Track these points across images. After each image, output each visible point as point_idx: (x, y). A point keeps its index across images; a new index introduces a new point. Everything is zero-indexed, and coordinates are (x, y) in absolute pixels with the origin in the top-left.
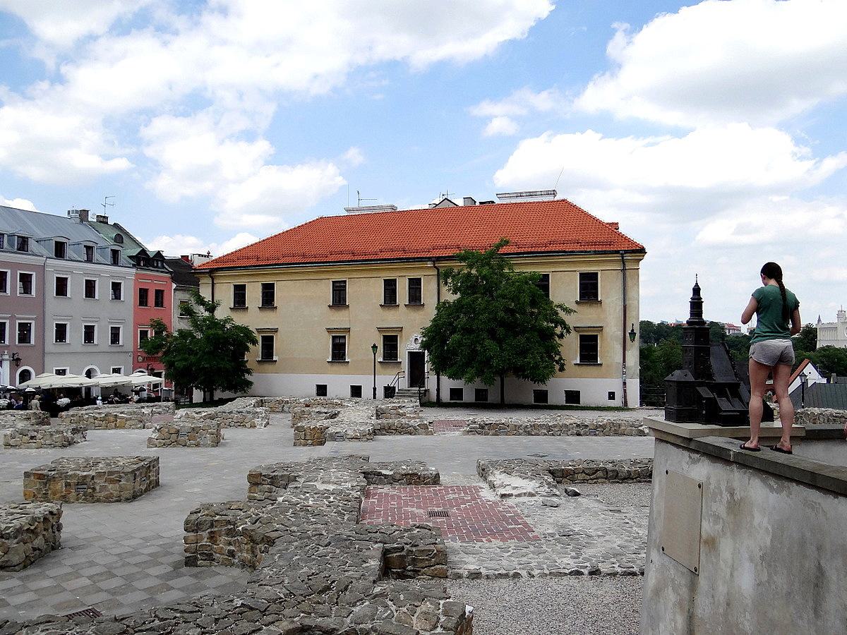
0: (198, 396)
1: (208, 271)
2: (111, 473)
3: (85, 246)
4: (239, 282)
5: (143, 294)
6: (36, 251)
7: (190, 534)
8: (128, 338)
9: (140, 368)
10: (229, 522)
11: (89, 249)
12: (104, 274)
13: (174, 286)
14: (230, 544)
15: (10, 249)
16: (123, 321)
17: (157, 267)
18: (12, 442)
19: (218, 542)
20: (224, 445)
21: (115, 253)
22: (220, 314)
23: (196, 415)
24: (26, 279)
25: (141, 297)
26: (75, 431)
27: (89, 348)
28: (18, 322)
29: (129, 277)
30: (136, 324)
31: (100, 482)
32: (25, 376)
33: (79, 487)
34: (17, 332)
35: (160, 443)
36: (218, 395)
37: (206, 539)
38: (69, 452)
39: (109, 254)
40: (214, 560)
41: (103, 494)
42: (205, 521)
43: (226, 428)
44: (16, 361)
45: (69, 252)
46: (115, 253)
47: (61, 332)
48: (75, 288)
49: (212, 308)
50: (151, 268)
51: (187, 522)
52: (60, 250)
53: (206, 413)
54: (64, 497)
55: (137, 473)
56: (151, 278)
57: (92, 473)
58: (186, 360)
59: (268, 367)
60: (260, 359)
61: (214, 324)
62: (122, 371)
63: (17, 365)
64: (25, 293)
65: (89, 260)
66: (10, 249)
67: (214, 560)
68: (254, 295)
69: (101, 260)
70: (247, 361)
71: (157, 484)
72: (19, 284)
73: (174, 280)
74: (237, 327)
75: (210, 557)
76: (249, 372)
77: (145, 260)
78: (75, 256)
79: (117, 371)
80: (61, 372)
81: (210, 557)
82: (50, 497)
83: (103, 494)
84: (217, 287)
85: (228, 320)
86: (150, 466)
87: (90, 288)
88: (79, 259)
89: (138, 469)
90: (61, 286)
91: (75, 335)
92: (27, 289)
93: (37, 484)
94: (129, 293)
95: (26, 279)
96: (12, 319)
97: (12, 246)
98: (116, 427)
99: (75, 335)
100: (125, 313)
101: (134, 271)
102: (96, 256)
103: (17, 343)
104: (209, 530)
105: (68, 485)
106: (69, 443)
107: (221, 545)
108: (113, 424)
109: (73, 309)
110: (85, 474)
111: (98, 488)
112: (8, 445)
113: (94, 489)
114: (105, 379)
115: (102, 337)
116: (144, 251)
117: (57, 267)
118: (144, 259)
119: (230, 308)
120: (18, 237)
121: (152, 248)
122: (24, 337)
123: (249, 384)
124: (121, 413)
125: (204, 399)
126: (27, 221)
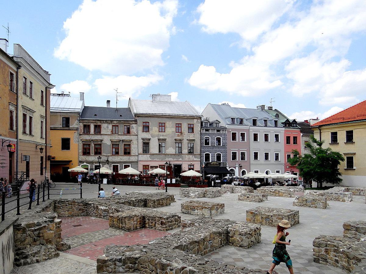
0: (314, 184)
1: (318, 126)
2: (279, 215)
3: (264, 120)
4: (334, 131)
5: (288, 139)
6: (246, 124)
7: (315, 248)
8: (282, 158)
9: (288, 171)
10: (335, 246)
11: (265, 121)
12: (272, 131)
13: (302, 134)
14: (336, 256)
15: (237, 124)
16: (280, 151)
17: (294, 126)
18: (241, 198)
19: (330, 254)
20: (329, 208)
21: (276, 122)
22: (324, 147)
23: (314, 193)
24: (243, 135)
25: (287, 140)
26: (263, 196)
27: (267, 162)
28: (241, 152)
29: (282, 132)
30: (286, 152)
31: (274, 218)
32: (244, 173)
33: (267, 219)
34: (241, 156)
35: (298, 204)
36: (324, 184)
37: (323, 252)
38: (261, 204)
39: (274, 122)
40: (328, 262)
41: (276, 223)
42: (323, 243)
43: (330, 200)
44: (241, 167)
45: (258, 123)
46: (276, 122)
47: (256, 155)
48: (261, 138)
49: (320, 144)
50: (292, 127)
51: (314, 242)
52: (254, 122)
53: (319, 193)
54: (261, 222)
55: (290, 217)
56: (292, 132)
57: (271, 214)
58: (308, 168)
59: (350, 172)
60: (346, 168)
61: (321, 151)
62: (280, 172)
63: (241, 169)
64: (243, 140)
65: (266, 126)
66: (237, 124)
67: (328, 262)
68: (342, 137)
69: (270, 125)
70: (339, 169)
71: (298, 223)
72: (241, 137)
73: (301, 132)
74: (333, 153)
75: (326, 260)
76: (340, 174)
77: (288, 124)
78: (260, 124)
79: (278, 172)
80: (257, 172)
81: (326, 260)
82: (256, 222)
83: (276, 223)
84: (322, 134)
85: (328, 150)
86: (295, 215)
87: (266, 137)
88: (262, 126)
89: (290, 215)
90: (256, 137)
91: (261, 157)
92: (243, 139)
93: (251, 216)
94: (282, 139)
95: (243, 135)
96: (239, 150)
97: (238, 123)
98: (279, 196)
99: (261, 157)
100: (281, 147)
101: (284, 129)
102: (269, 124)
103: (240, 160)
104: (325, 248)
105: (262, 218)
106: (262, 201)
107: (331, 256)
108: (278, 194)
109: (260, 147)
110: (268, 214)
111: (274, 221)
112: (239, 199)
113: (272, 221)
114: (273, 175)
115: (272, 157)
116: (288, 120)
117: (254, 130)
118: (288, 124)
119: (330, 144)
120: (240, 119)
121: (291, 118)
122: (243, 158)
123: (340, 180)
124: (281, 190)
125: (318, 186)
126: (243, 113)
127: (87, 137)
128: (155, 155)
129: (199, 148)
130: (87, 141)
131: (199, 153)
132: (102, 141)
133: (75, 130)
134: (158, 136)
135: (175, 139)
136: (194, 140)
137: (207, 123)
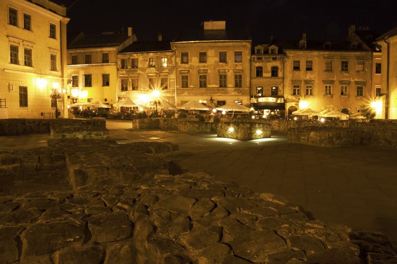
129: (248, 79)
131: (248, 84)
134: (199, 66)
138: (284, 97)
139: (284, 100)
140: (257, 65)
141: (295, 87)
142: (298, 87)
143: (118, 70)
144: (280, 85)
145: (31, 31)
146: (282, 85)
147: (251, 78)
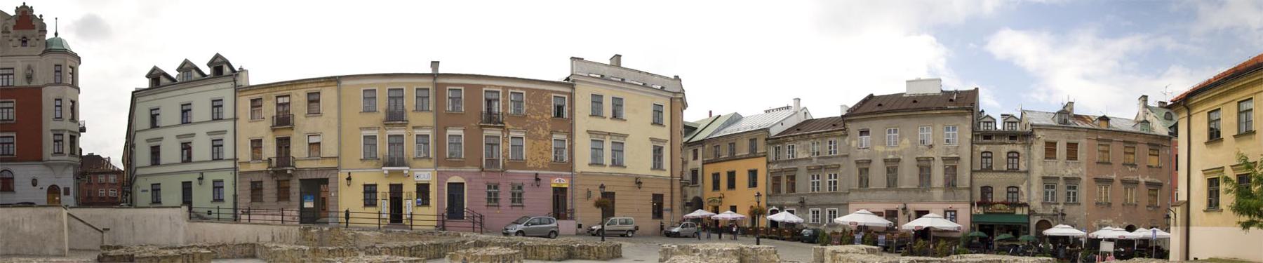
127: (775, 167)
128: (878, 192)
129: (967, 174)
130: (775, 172)
131: (968, 186)
132: (796, 169)
133: (762, 156)
135: (917, 158)
136: (958, 159)
137: (991, 122)
138: (1029, 206)
139: (1029, 210)
140: (983, 148)
141: (1047, 187)
142: (1053, 187)
143: (768, 163)
144: (1022, 184)
145: (622, 119)
146: (1025, 184)
147: (973, 171)
